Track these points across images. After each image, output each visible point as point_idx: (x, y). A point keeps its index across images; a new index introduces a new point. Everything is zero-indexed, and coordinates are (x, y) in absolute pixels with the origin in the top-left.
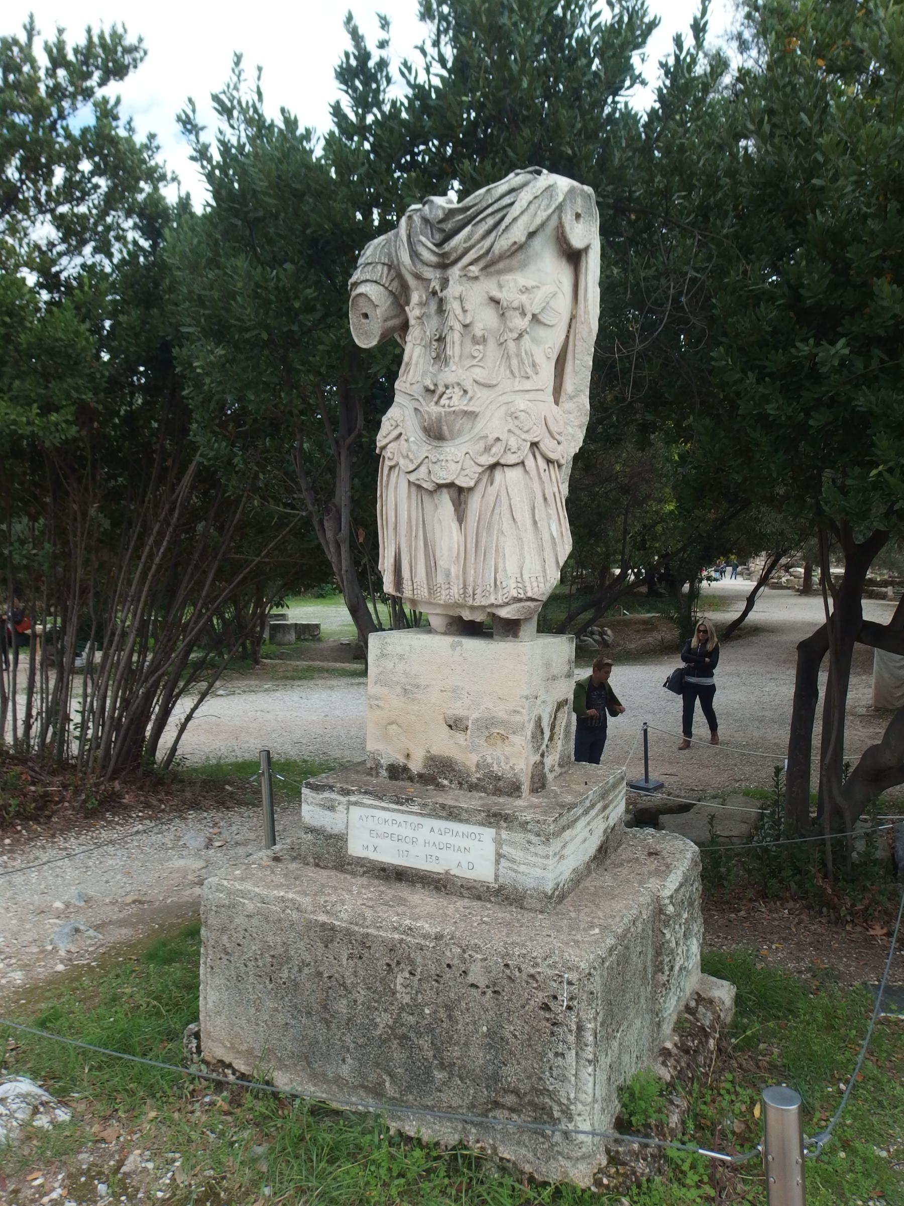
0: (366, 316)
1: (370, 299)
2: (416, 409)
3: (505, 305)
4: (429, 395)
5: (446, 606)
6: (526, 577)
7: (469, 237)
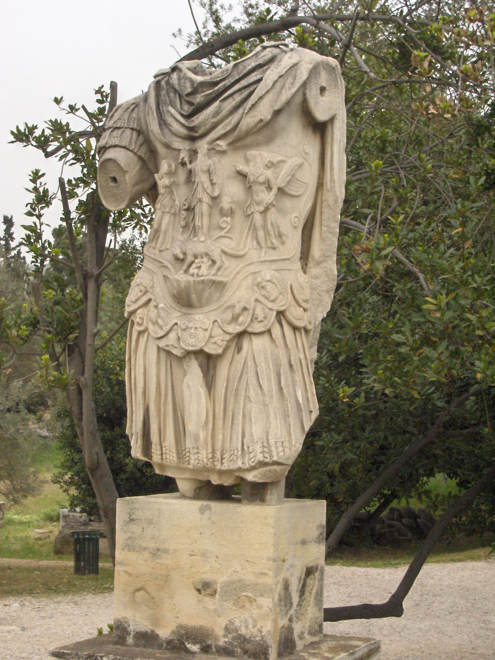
0: (114, 180)
1: (119, 165)
2: (165, 277)
3: (252, 178)
4: (178, 265)
5: (194, 471)
6: (272, 441)
7: (217, 113)
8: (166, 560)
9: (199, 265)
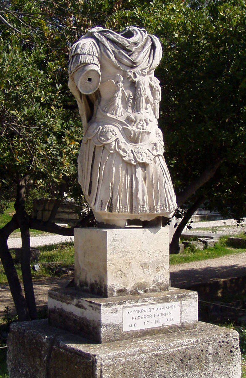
8: (129, 256)
9: (142, 124)
